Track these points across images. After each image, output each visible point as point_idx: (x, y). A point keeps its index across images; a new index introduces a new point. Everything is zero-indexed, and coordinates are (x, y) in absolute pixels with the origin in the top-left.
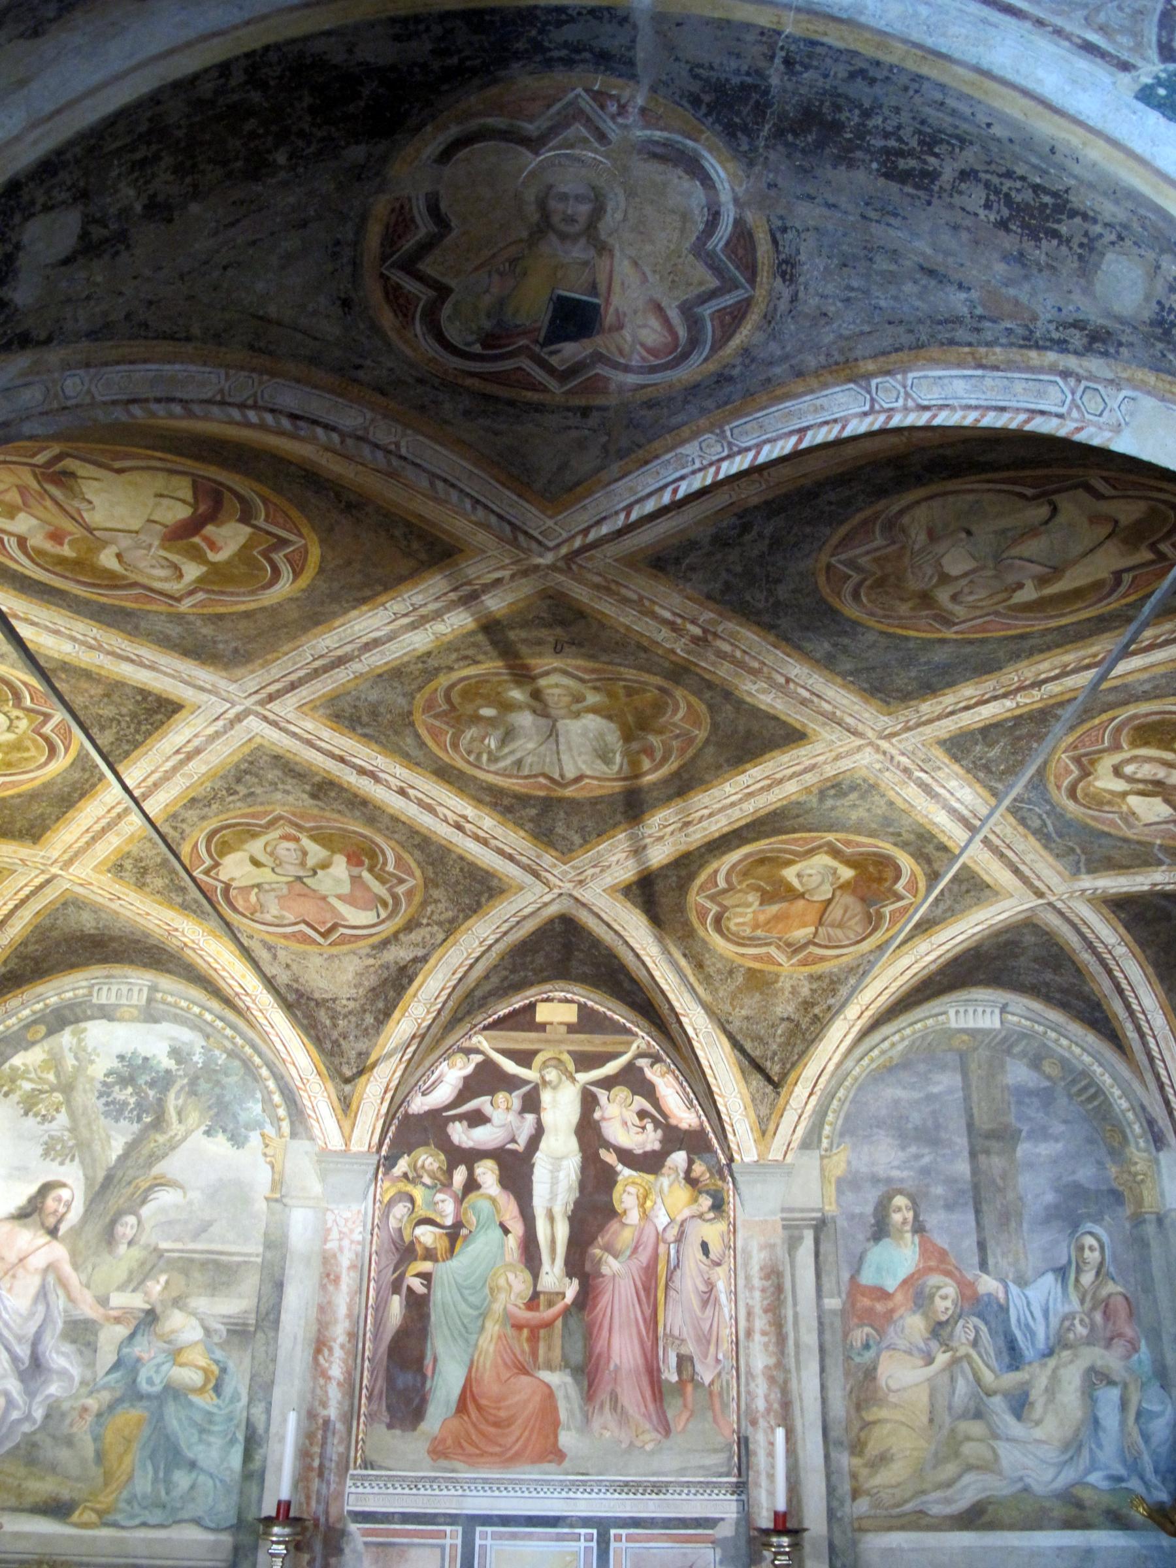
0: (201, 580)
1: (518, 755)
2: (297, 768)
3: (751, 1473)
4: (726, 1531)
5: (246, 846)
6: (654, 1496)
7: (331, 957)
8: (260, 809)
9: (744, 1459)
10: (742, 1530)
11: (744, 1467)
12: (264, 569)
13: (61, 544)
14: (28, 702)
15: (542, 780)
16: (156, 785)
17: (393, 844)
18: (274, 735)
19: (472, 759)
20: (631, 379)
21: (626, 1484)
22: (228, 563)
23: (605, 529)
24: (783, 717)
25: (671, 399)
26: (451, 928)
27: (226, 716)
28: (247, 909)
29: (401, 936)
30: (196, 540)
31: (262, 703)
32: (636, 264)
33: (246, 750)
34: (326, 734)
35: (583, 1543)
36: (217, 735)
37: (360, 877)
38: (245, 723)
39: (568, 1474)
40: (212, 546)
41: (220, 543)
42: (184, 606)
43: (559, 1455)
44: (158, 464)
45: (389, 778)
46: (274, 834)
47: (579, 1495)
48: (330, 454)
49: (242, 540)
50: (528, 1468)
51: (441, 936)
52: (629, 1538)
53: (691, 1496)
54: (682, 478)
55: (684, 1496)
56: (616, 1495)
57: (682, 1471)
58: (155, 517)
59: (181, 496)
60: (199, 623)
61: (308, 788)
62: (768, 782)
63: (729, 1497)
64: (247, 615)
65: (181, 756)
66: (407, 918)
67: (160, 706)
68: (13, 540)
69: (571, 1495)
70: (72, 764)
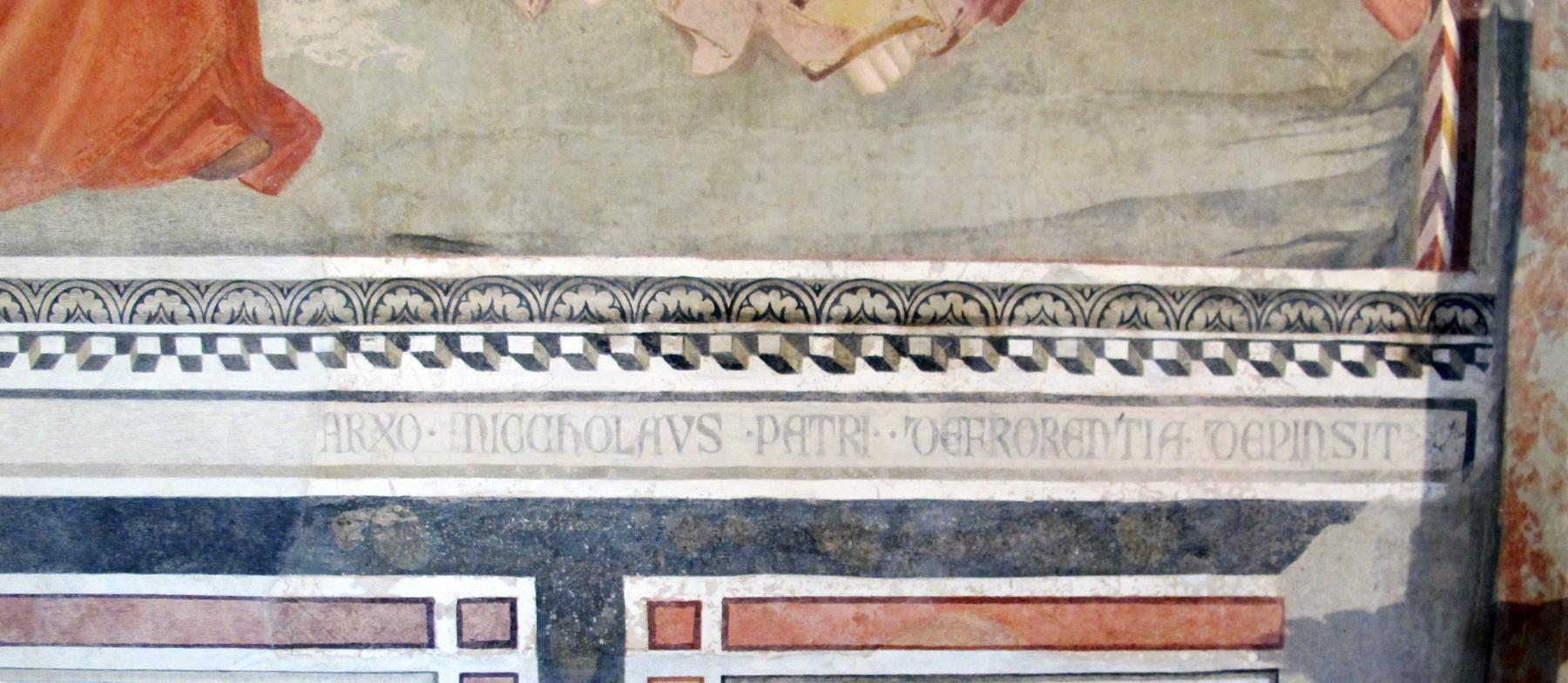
3: (1529, 243)
4: (1357, 580)
6: (907, 377)
9: (1492, 158)
10: (1448, 575)
11: (1488, 206)
21: (727, 303)
35: (448, 658)
39: (332, 246)
43: (264, 128)
47: (409, 374)
50: (67, 211)
52: (746, 627)
53: (1152, 380)
55: (1103, 378)
56: (659, 375)
57: (1105, 221)
63: (1384, 382)
69: (359, 373)
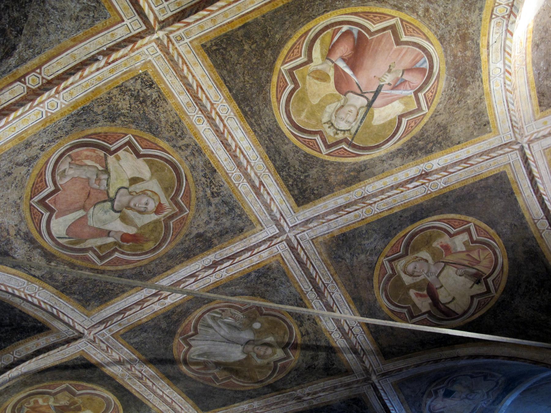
0: (400, 278)
1: (217, 328)
2: (228, 236)
5: (155, 181)
7: (18, 207)
8: (194, 202)
12: (399, 302)
13: (442, 246)
14: (344, 146)
15: (192, 332)
16: (235, 157)
17: (146, 262)
18: (262, 236)
19: (217, 310)
20: (428, 403)
22: (408, 294)
23: (383, 394)
24: (224, 408)
25: (420, 409)
26: (48, 279)
27: (282, 220)
28: (78, 154)
29: (39, 250)
30: (425, 292)
31: (288, 241)
32: (456, 404)
33: (252, 218)
34: (255, 260)
36: (270, 212)
37: (108, 235)
38: (274, 226)
40: (421, 296)
41: (419, 298)
42: (383, 260)
44: (472, 311)
45: (206, 274)
46: (165, 201)
48: (456, 356)
49: (419, 306)
51: (38, 273)
54: (395, 411)
58: (442, 289)
59: (450, 304)
60: (370, 258)
61: (210, 235)
62: (170, 401)
64: (370, 279)
65: (257, 184)
66: (58, 255)
67: (304, 197)
68: (452, 233)
70: (279, 129)
